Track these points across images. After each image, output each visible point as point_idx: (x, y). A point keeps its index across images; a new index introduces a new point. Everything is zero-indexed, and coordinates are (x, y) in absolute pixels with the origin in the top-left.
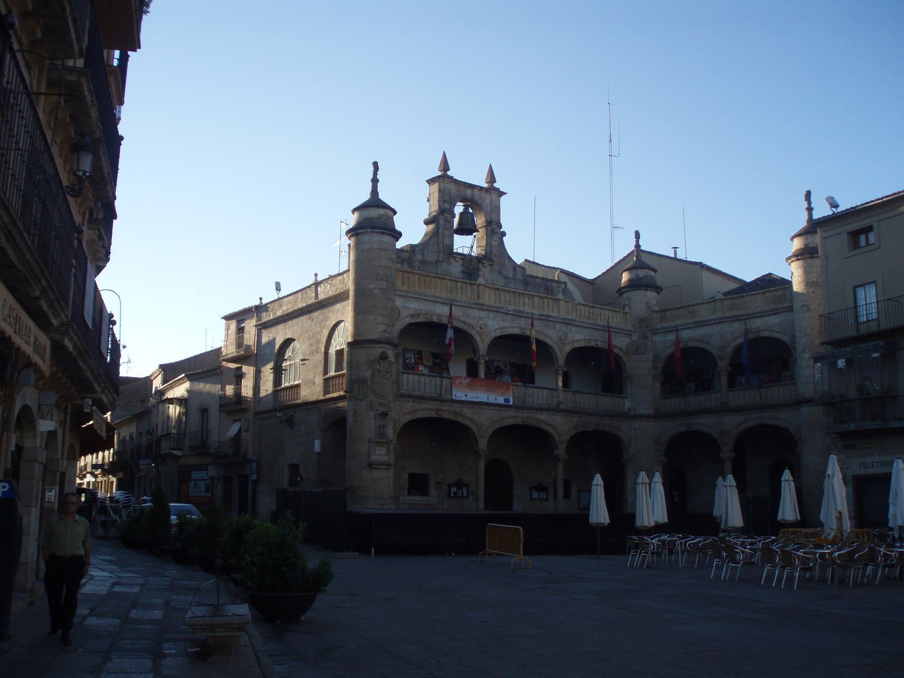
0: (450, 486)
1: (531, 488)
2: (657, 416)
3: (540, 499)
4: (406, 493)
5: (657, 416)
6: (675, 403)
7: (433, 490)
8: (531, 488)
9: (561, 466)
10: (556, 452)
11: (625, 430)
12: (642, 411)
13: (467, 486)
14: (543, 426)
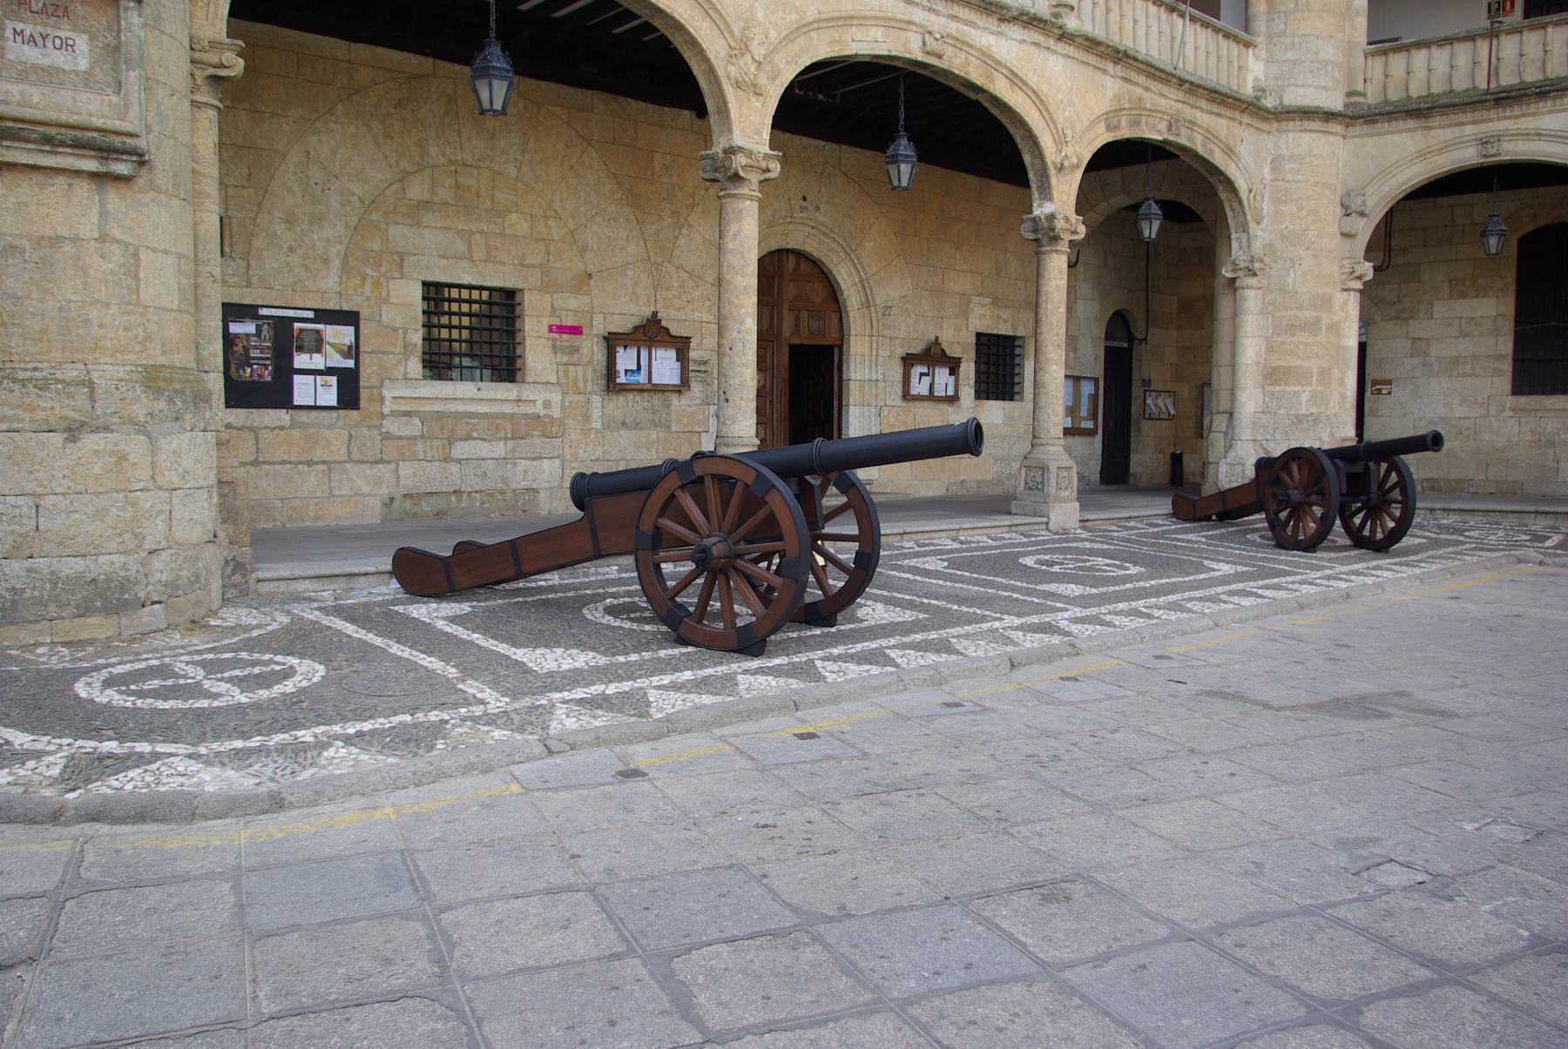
0: (612, 342)
1: (909, 361)
2: (1358, 116)
3: (931, 397)
4: (415, 366)
5: (1358, 116)
6: (1429, 70)
7: (537, 351)
8: (909, 361)
9: (1056, 266)
10: (1041, 210)
11: (1245, 157)
12: (1297, 97)
13: (682, 346)
14: (1001, 88)
